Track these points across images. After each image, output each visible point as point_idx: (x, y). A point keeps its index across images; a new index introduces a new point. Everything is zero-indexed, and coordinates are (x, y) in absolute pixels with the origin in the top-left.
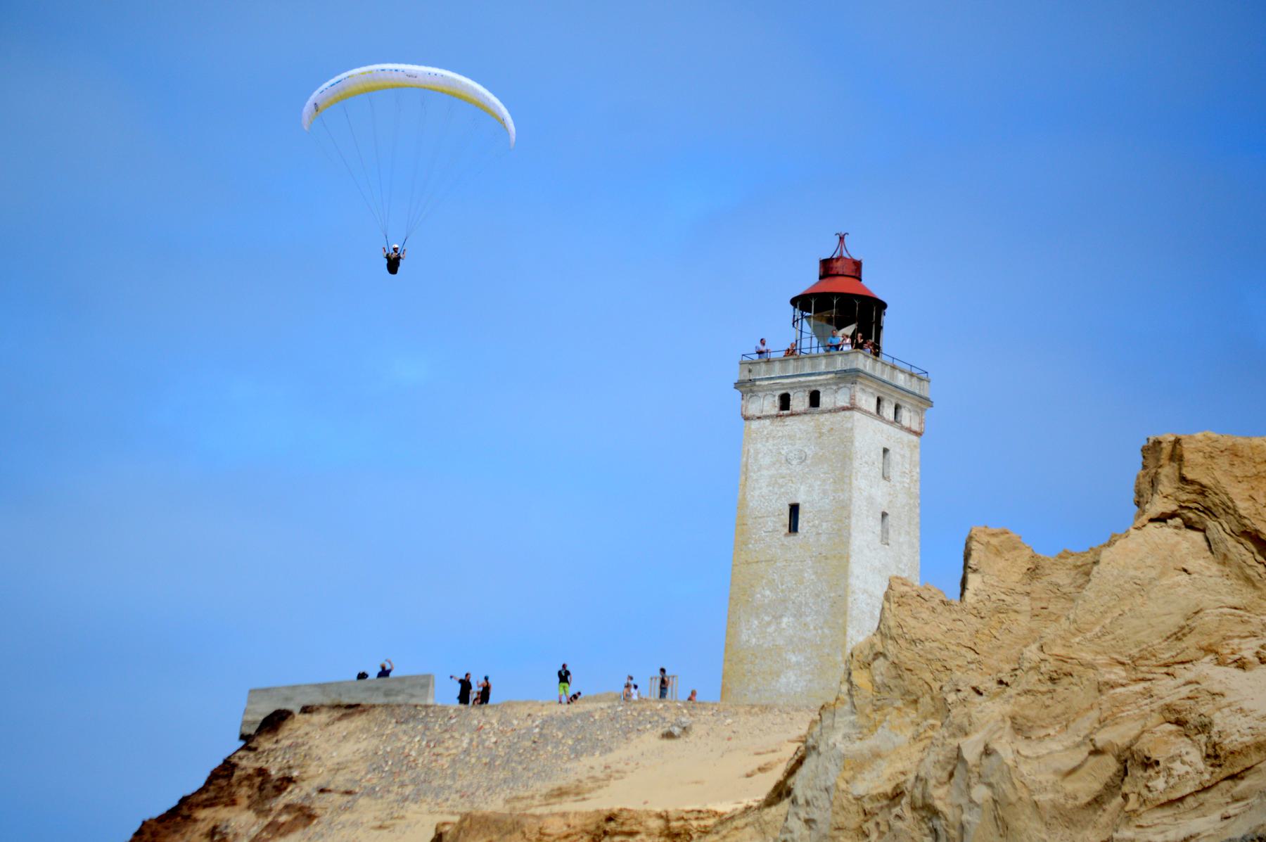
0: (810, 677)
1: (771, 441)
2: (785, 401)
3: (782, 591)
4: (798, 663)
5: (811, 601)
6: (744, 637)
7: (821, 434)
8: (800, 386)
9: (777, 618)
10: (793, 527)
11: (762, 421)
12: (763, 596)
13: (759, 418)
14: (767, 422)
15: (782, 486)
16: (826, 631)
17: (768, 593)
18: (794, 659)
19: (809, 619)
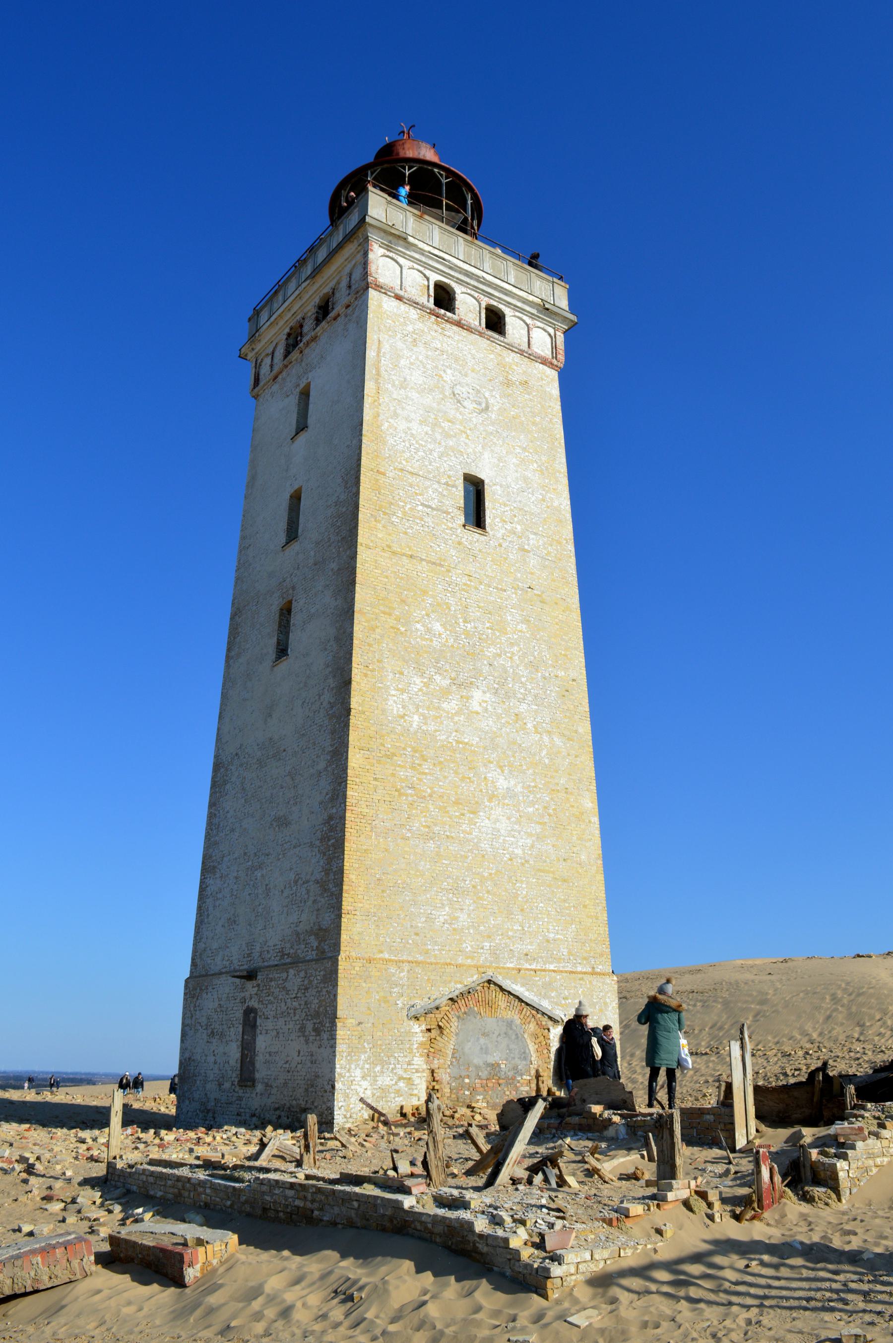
0: (538, 828)
1: (421, 348)
2: (444, 298)
3: (467, 633)
4: (510, 793)
5: (522, 671)
6: (394, 706)
7: (508, 383)
8: (478, 285)
9: (463, 685)
10: (476, 515)
11: (403, 307)
12: (429, 631)
13: (399, 298)
14: (413, 313)
15: (447, 436)
16: (558, 741)
17: (437, 627)
18: (502, 783)
19: (523, 707)
